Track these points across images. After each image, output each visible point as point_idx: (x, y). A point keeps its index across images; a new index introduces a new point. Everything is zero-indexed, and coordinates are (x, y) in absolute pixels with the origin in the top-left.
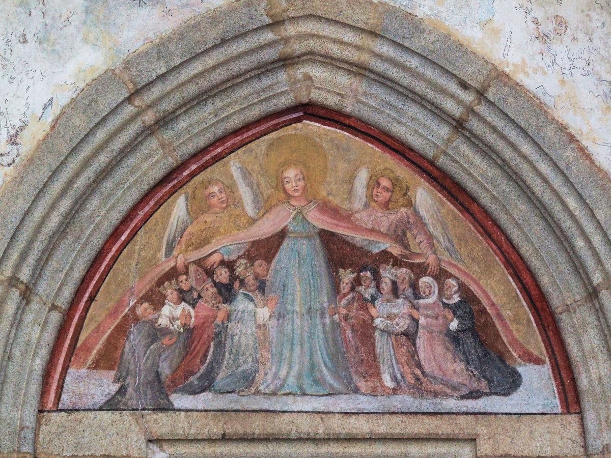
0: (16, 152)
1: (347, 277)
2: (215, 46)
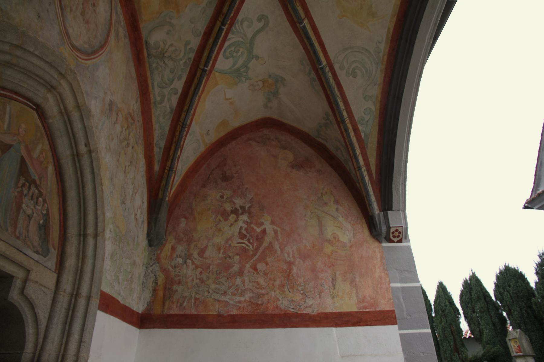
1: (22, 181)
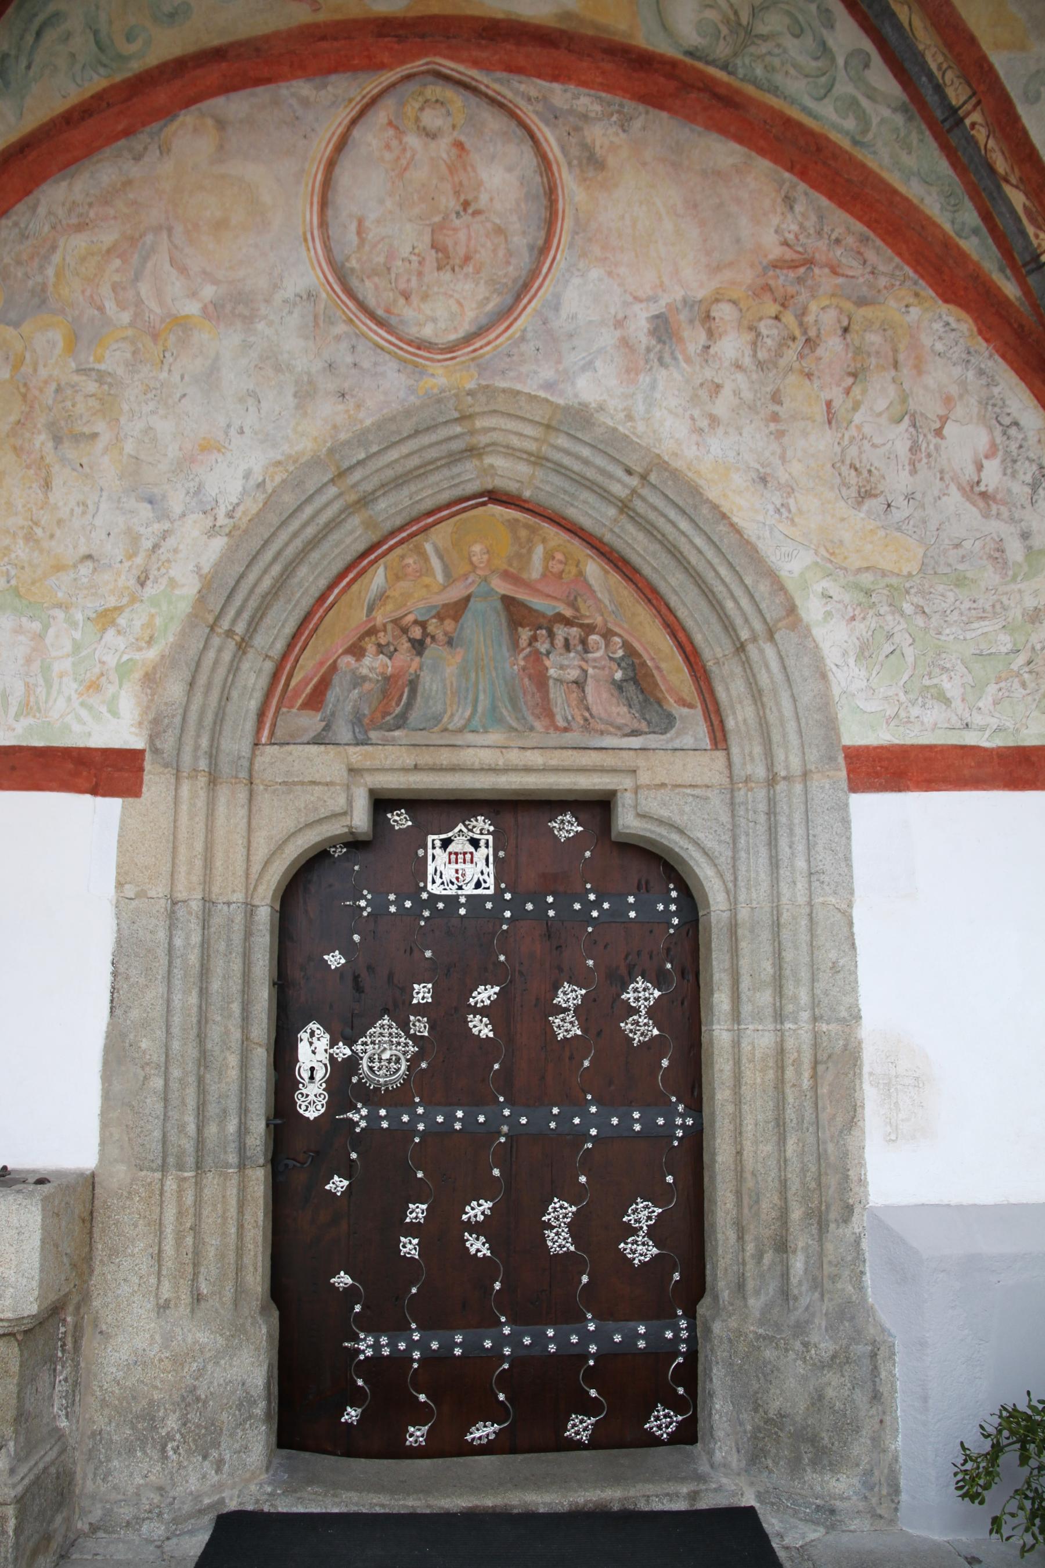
1: (525, 634)
2: (409, 437)
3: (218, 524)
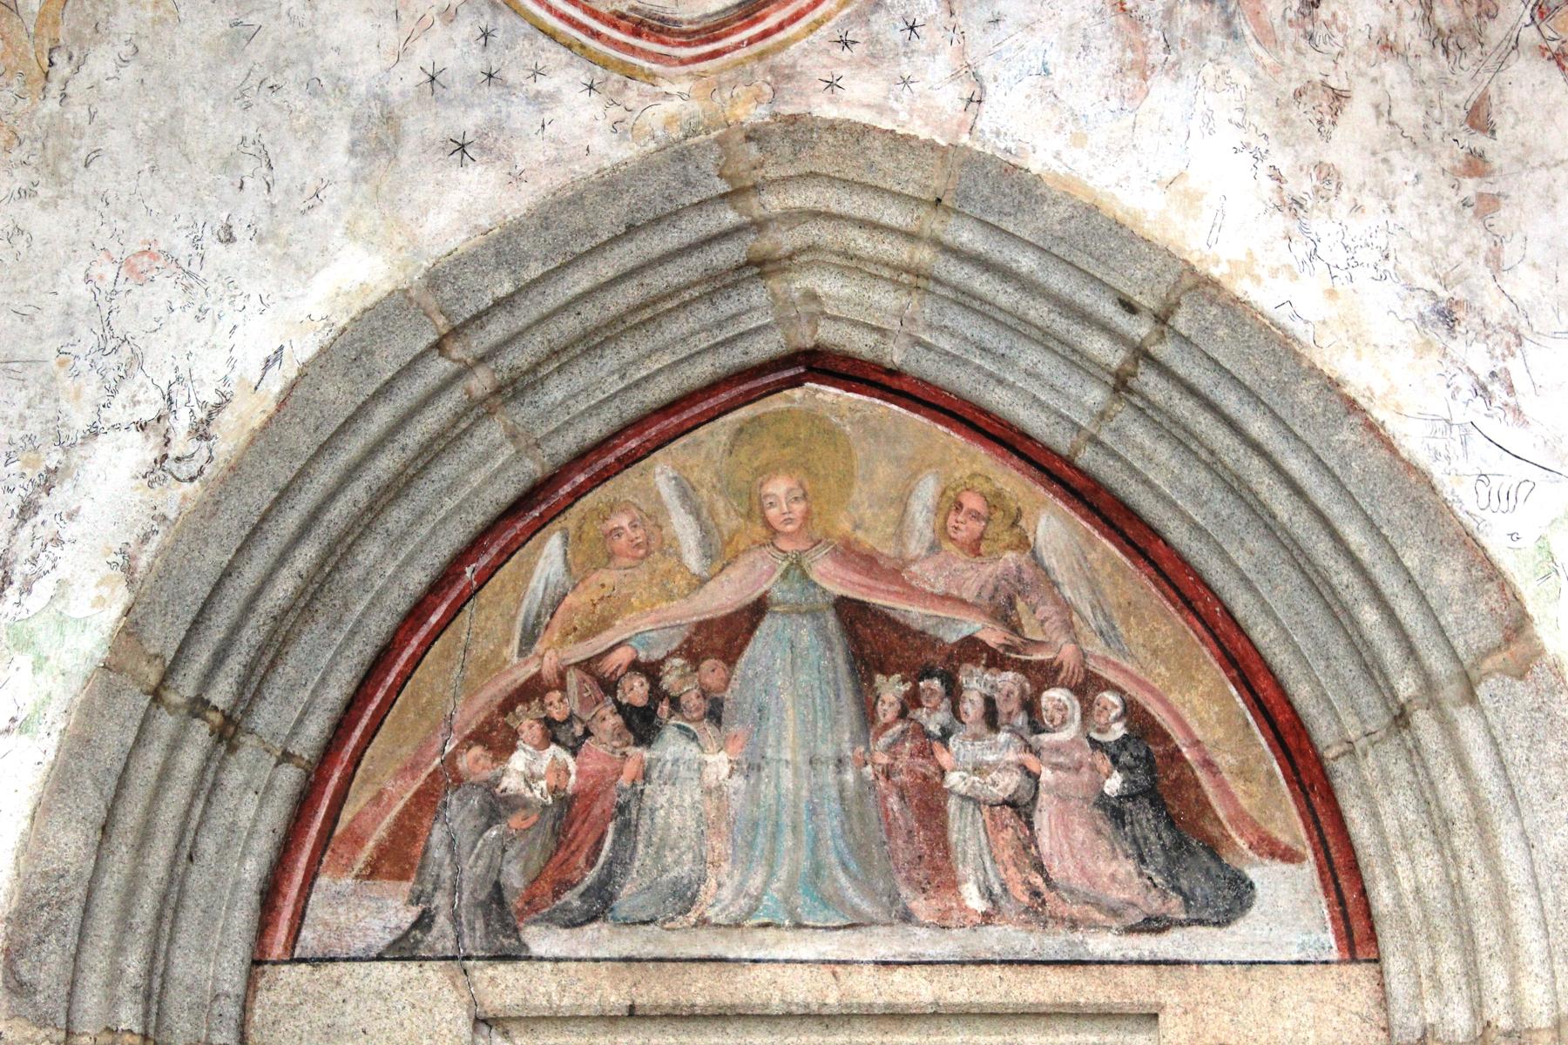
0: (206, 454)
1: (891, 690)
2: (615, 240)
3: (172, 454)
